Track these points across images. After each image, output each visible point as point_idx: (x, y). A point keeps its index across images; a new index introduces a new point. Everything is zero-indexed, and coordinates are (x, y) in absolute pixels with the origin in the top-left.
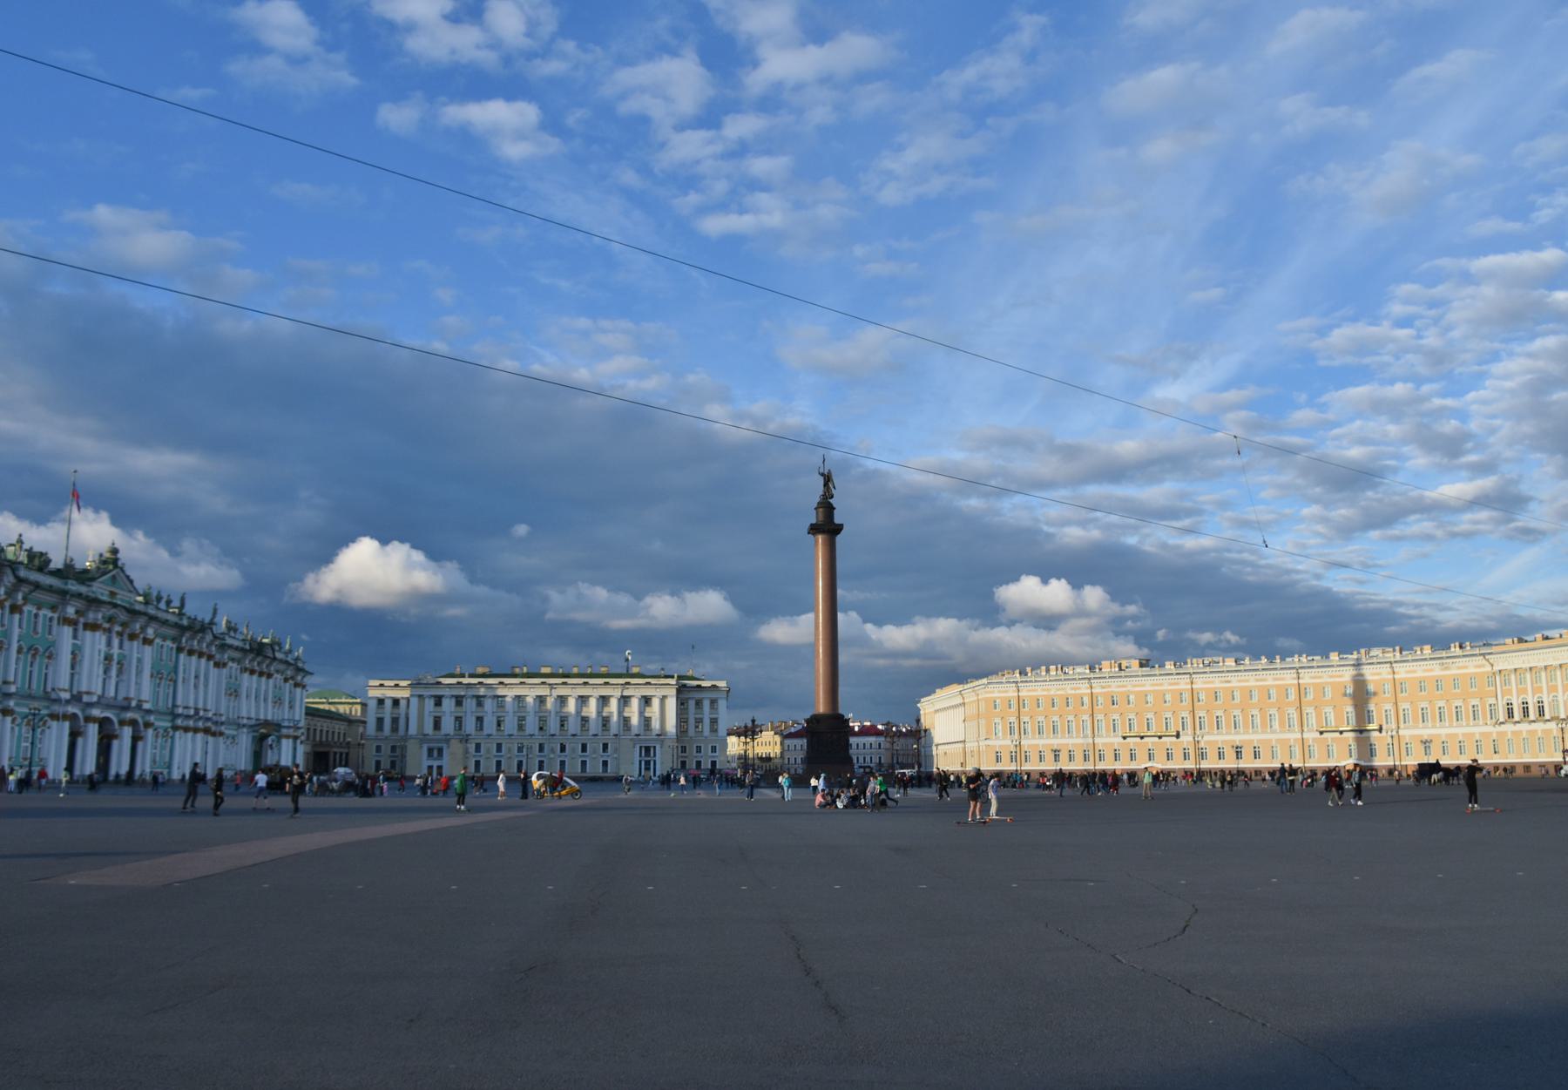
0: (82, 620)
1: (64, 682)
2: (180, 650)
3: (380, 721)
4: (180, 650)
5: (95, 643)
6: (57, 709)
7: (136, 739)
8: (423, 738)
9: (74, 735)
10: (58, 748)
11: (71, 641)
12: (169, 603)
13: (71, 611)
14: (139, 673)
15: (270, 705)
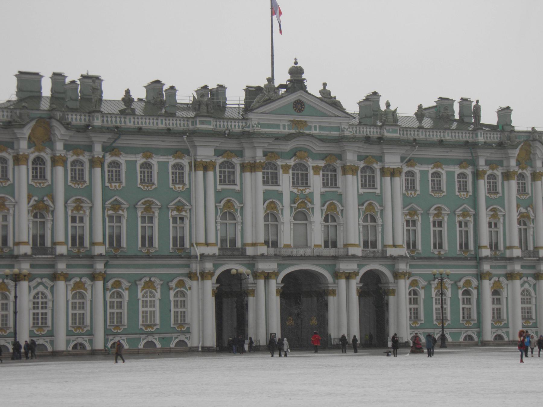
0: (236, 161)
2: (477, 175)
4: (477, 175)
6: (195, 267)
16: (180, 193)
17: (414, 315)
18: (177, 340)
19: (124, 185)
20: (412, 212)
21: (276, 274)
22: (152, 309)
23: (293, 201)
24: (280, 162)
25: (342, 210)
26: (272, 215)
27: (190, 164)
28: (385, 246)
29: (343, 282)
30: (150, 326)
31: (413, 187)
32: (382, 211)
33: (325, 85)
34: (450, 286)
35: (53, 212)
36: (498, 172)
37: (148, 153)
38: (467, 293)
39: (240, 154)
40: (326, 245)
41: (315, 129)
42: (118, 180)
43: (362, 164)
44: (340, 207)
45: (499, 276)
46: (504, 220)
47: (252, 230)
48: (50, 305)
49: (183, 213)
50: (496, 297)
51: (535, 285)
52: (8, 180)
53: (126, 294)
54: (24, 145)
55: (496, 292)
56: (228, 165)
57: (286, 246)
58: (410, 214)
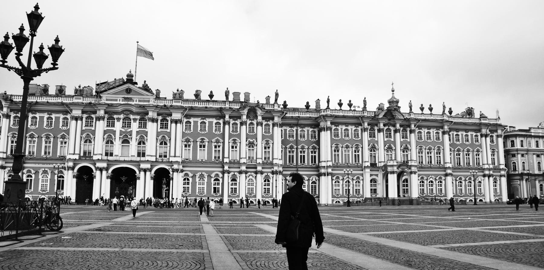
0: (93, 116)
4: (224, 123)
13: (77, 112)
16: (64, 131)
17: (185, 190)
20: (188, 141)
21: (107, 169)
23: (121, 135)
24: (115, 116)
26: (109, 141)
29: (142, 173)
30: (43, 191)
31: (190, 129)
32: (170, 139)
33: (145, 82)
34: (206, 177)
36: (238, 122)
37: (50, 112)
38: (217, 180)
39: (95, 112)
40: (139, 155)
41: (136, 101)
42: (36, 125)
43: (160, 118)
44: (145, 137)
45: (234, 172)
46: (240, 145)
47: (98, 147)
50: (234, 182)
51: (256, 177)
53: (33, 176)
55: (234, 180)
57: (115, 155)
58: (186, 141)
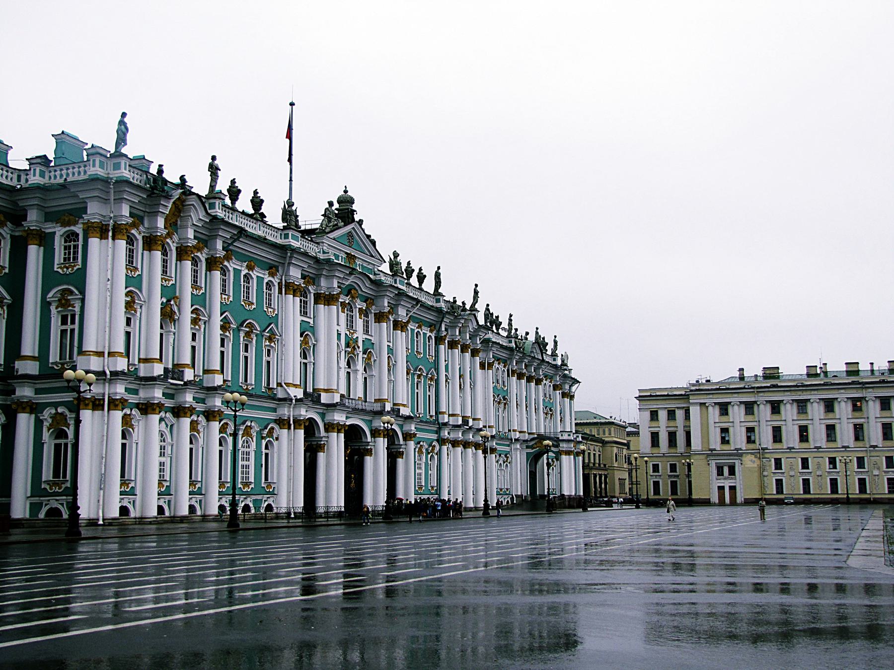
0: (311, 288)
1: (293, 374)
2: (439, 340)
3: (655, 437)
4: (439, 340)
5: (331, 322)
6: (286, 412)
7: (393, 456)
8: (711, 454)
9: (313, 449)
10: (291, 467)
11: (300, 318)
12: (421, 278)
13: (295, 274)
14: (391, 368)
15: (542, 415)
18: (266, 503)
19: (231, 299)
22: (247, 463)
23: (347, 345)
25: (375, 361)
27: (280, 284)
28: (394, 404)
35: (175, 321)
48: (168, 450)
49: (272, 344)
52: (137, 269)
54: (161, 222)
56: (304, 293)
